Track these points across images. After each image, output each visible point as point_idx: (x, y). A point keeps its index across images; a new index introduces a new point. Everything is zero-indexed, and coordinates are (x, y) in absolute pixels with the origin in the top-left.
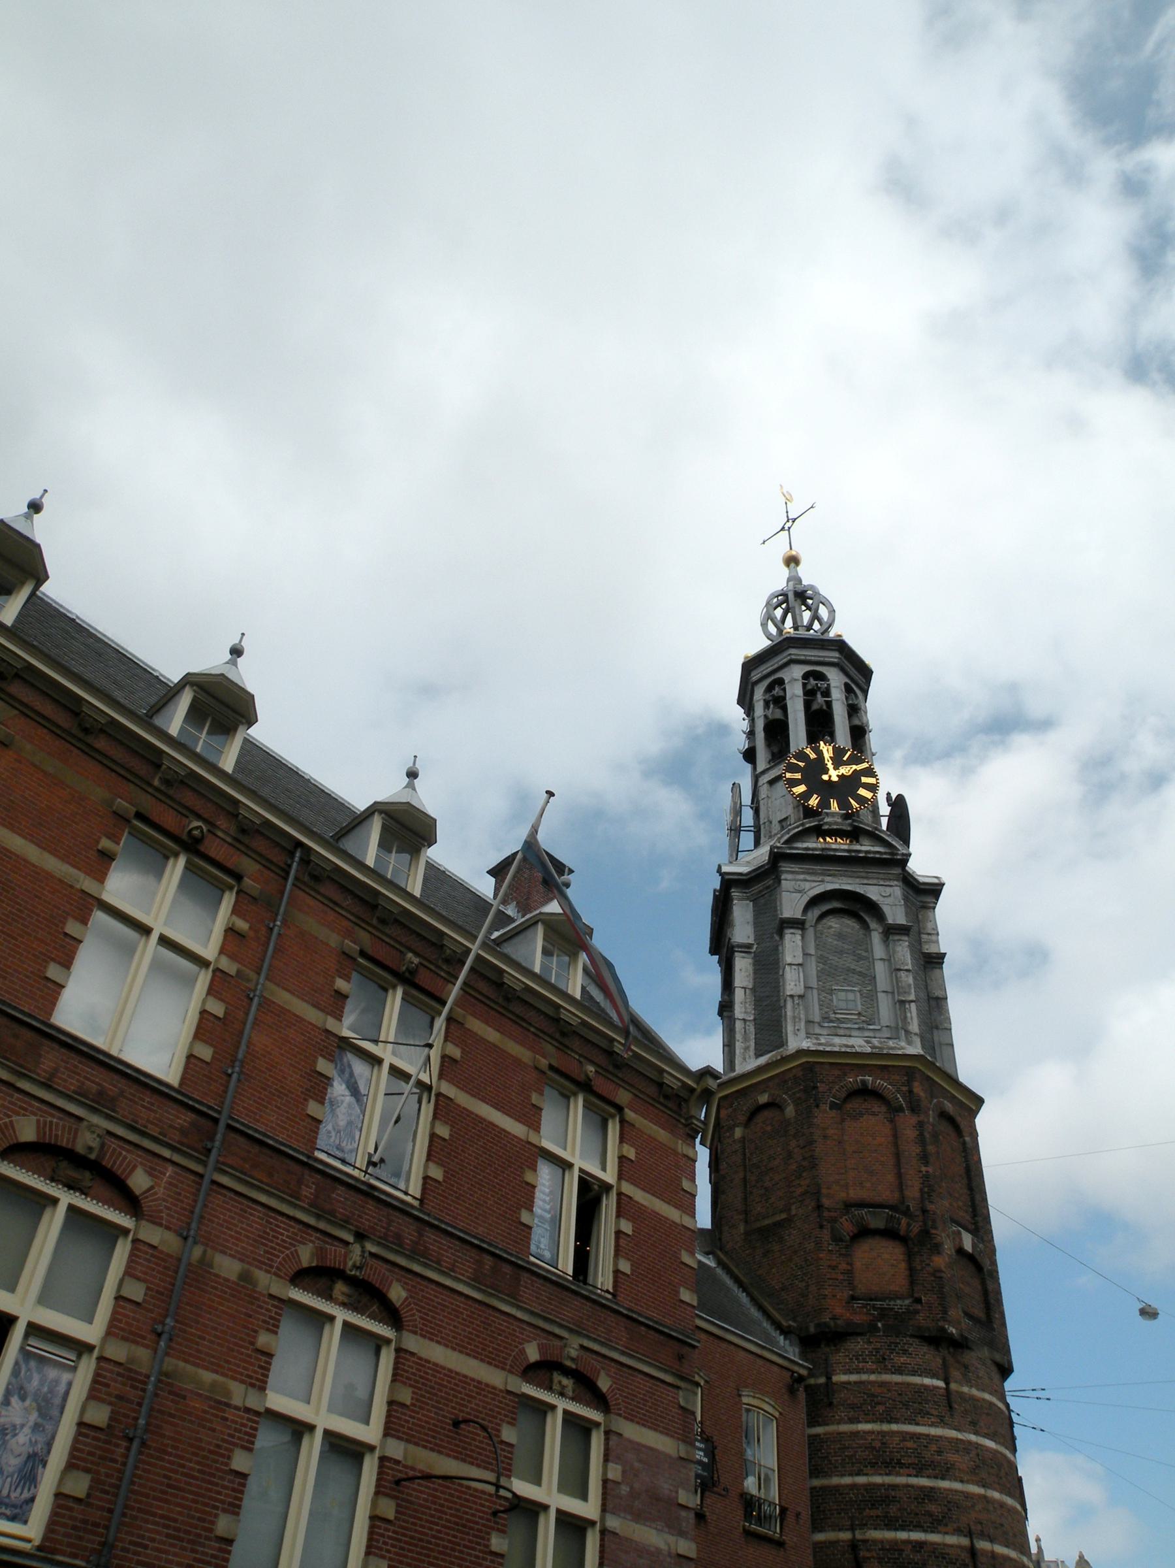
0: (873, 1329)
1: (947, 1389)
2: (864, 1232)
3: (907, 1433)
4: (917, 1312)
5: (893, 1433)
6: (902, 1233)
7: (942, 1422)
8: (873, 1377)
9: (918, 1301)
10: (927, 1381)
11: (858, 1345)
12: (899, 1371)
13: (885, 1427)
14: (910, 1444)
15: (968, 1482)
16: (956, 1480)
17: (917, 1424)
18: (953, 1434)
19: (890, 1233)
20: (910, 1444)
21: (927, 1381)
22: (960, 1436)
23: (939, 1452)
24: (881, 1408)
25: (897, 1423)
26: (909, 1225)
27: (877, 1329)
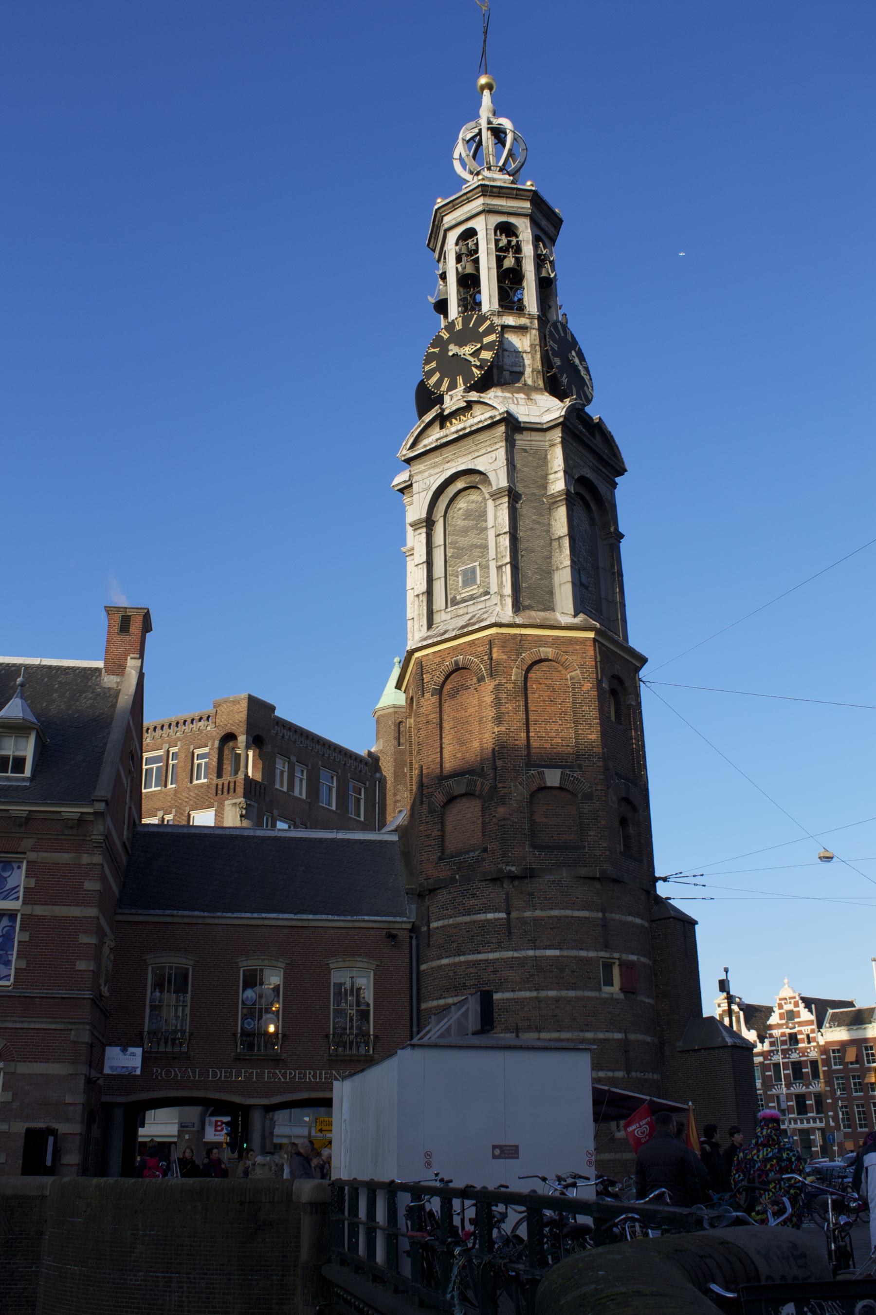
0: (453, 880)
1: (508, 919)
2: (452, 799)
3: (471, 961)
4: (484, 860)
5: (460, 963)
6: (477, 793)
7: (500, 947)
8: (451, 921)
9: (485, 850)
10: (490, 916)
11: (443, 896)
12: (468, 912)
13: (457, 959)
14: (473, 970)
15: (520, 990)
16: (508, 991)
17: (479, 953)
18: (510, 954)
19: (469, 794)
20: (473, 970)
21: (490, 916)
22: (516, 954)
23: (495, 972)
24: (454, 945)
25: (464, 955)
26: (482, 784)
27: (455, 881)
